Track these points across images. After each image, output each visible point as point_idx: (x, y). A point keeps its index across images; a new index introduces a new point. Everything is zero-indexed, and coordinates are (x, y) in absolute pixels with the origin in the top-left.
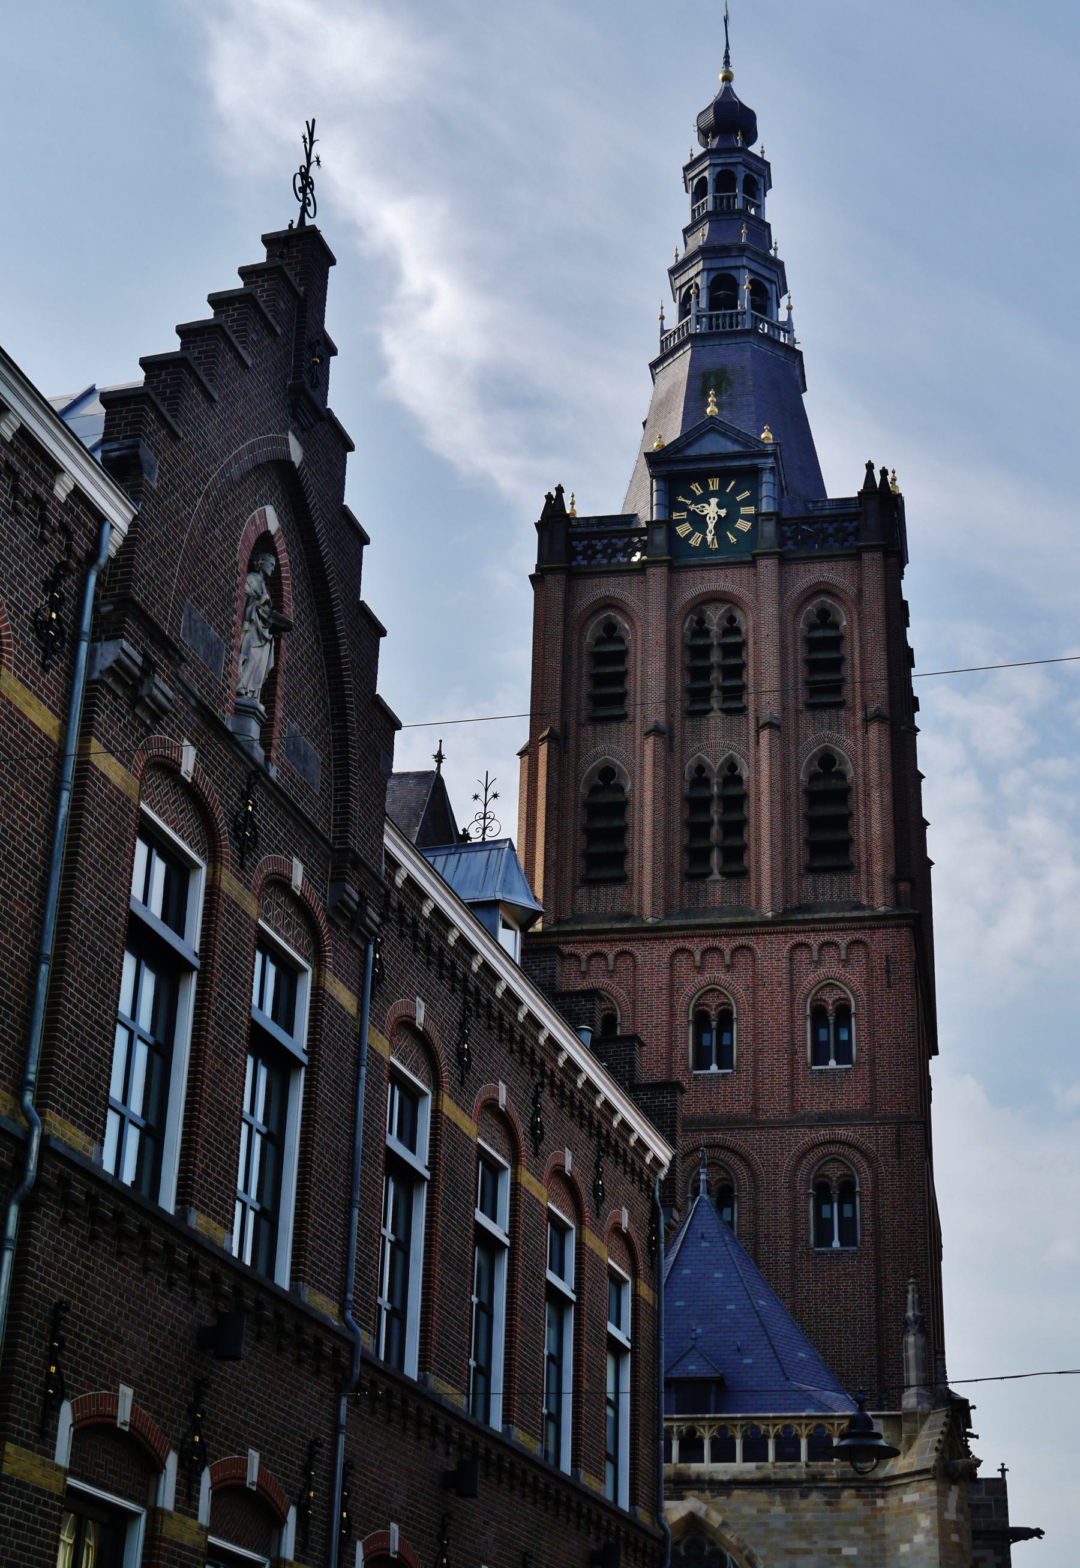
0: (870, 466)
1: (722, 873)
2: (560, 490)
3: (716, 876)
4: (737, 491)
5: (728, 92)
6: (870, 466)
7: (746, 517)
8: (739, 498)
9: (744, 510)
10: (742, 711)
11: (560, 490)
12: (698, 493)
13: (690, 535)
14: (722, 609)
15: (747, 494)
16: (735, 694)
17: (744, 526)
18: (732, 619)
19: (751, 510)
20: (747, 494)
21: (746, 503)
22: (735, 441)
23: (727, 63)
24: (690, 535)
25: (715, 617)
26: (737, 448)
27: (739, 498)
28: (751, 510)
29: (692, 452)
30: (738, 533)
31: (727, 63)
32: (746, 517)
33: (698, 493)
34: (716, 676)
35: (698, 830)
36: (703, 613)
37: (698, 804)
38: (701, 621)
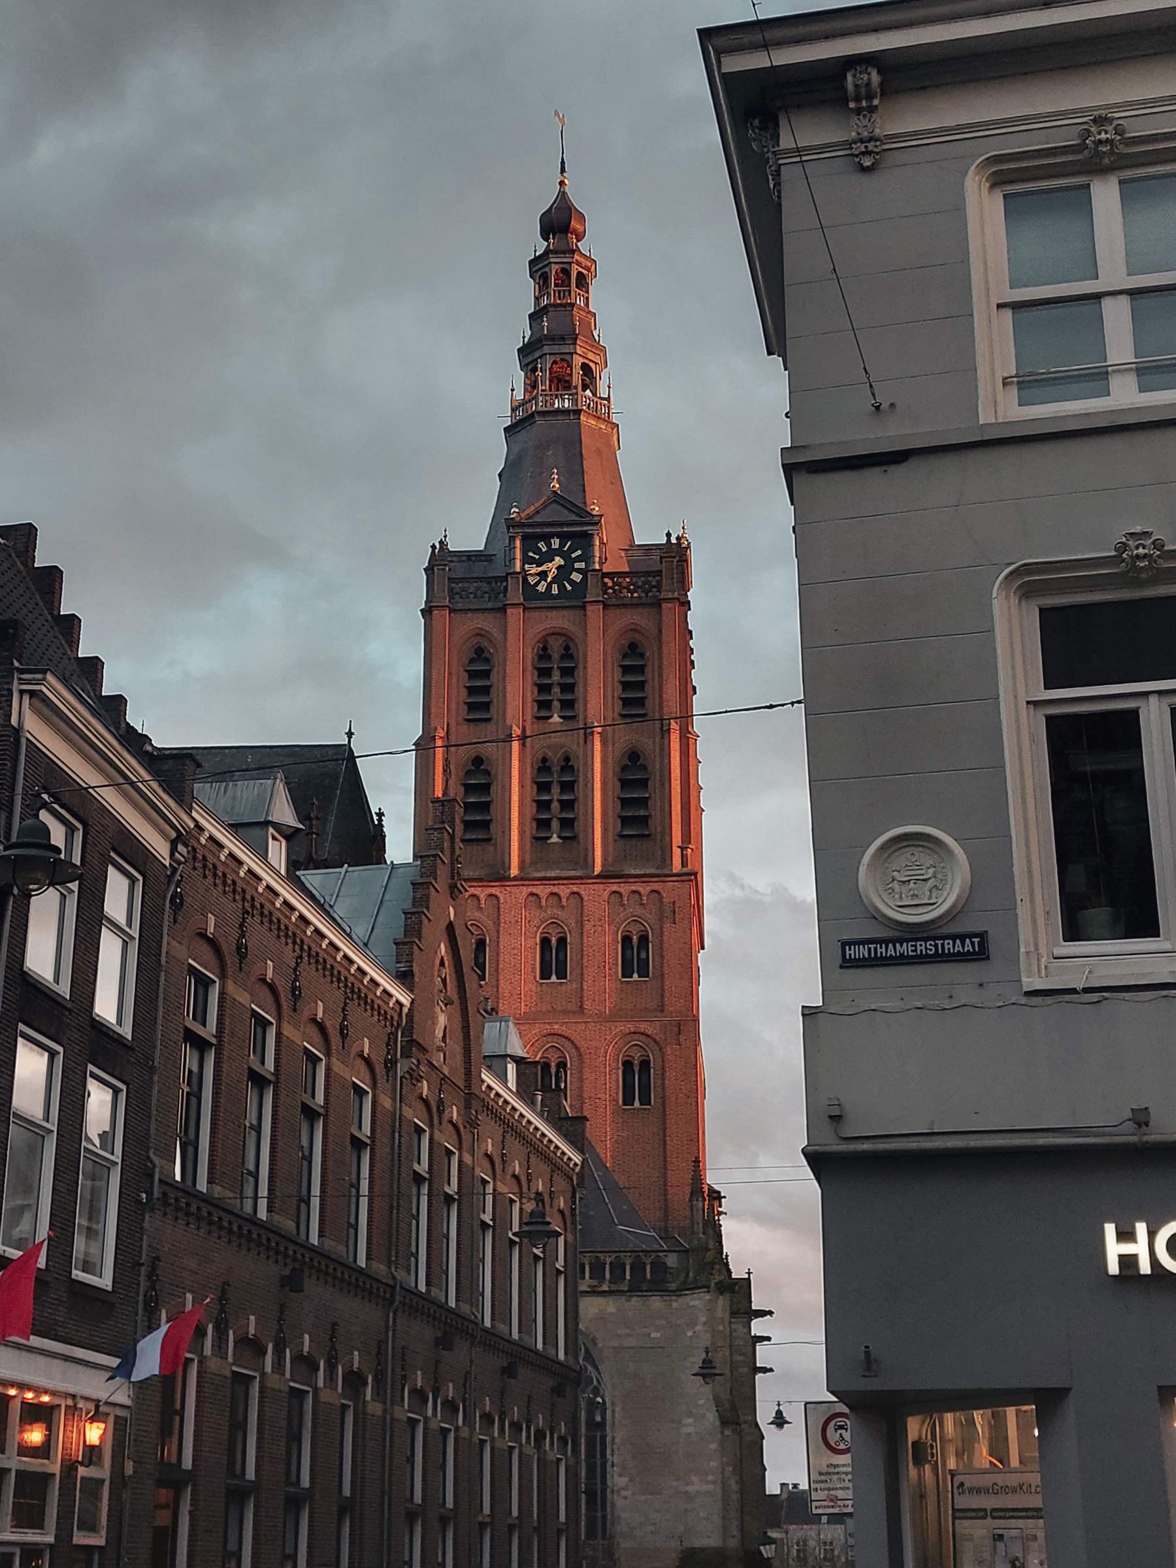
4: (572, 549)
5: (562, 195)
7: (579, 571)
8: (573, 556)
9: (577, 565)
12: (544, 550)
14: (561, 640)
15: (579, 552)
17: (576, 577)
18: (567, 648)
19: (582, 565)
20: (579, 552)
21: (578, 559)
23: (563, 170)
25: (556, 647)
26: (574, 517)
27: (573, 556)
28: (582, 565)
30: (572, 582)
31: (563, 170)
32: (579, 571)
33: (544, 550)
34: (556, 690)
36: (547, 642)
38: (545, 649)
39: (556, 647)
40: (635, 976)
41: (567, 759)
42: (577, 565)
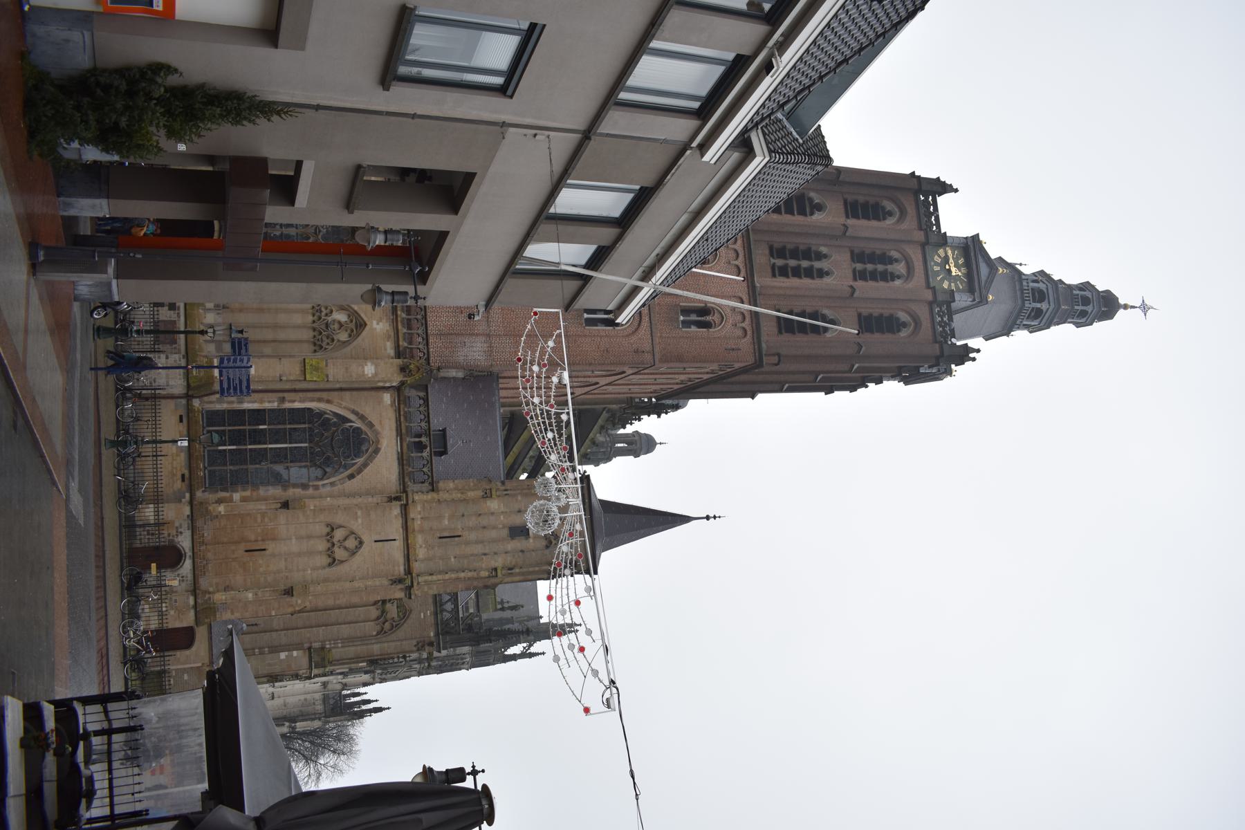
0: (978, 351)
1: (774, 264)
2: (956, 191)
3: (773, 261)
6: (978, 351)
7: (950, 285)
10: (855, 279)
11: (956, 191)
13: (939, 256)
15: (961, 287)
16: (860, 276)
18: (899, 277)
21: (956, 286)
22: (986, 281)
24: (939, 256)
29: (981, 260)
30: (942, 280)
35: (795, 254)
37: (807, 254)
39: (900, 268)
40: (682, 318)
41: (828, 274)
42: (953, 284)
